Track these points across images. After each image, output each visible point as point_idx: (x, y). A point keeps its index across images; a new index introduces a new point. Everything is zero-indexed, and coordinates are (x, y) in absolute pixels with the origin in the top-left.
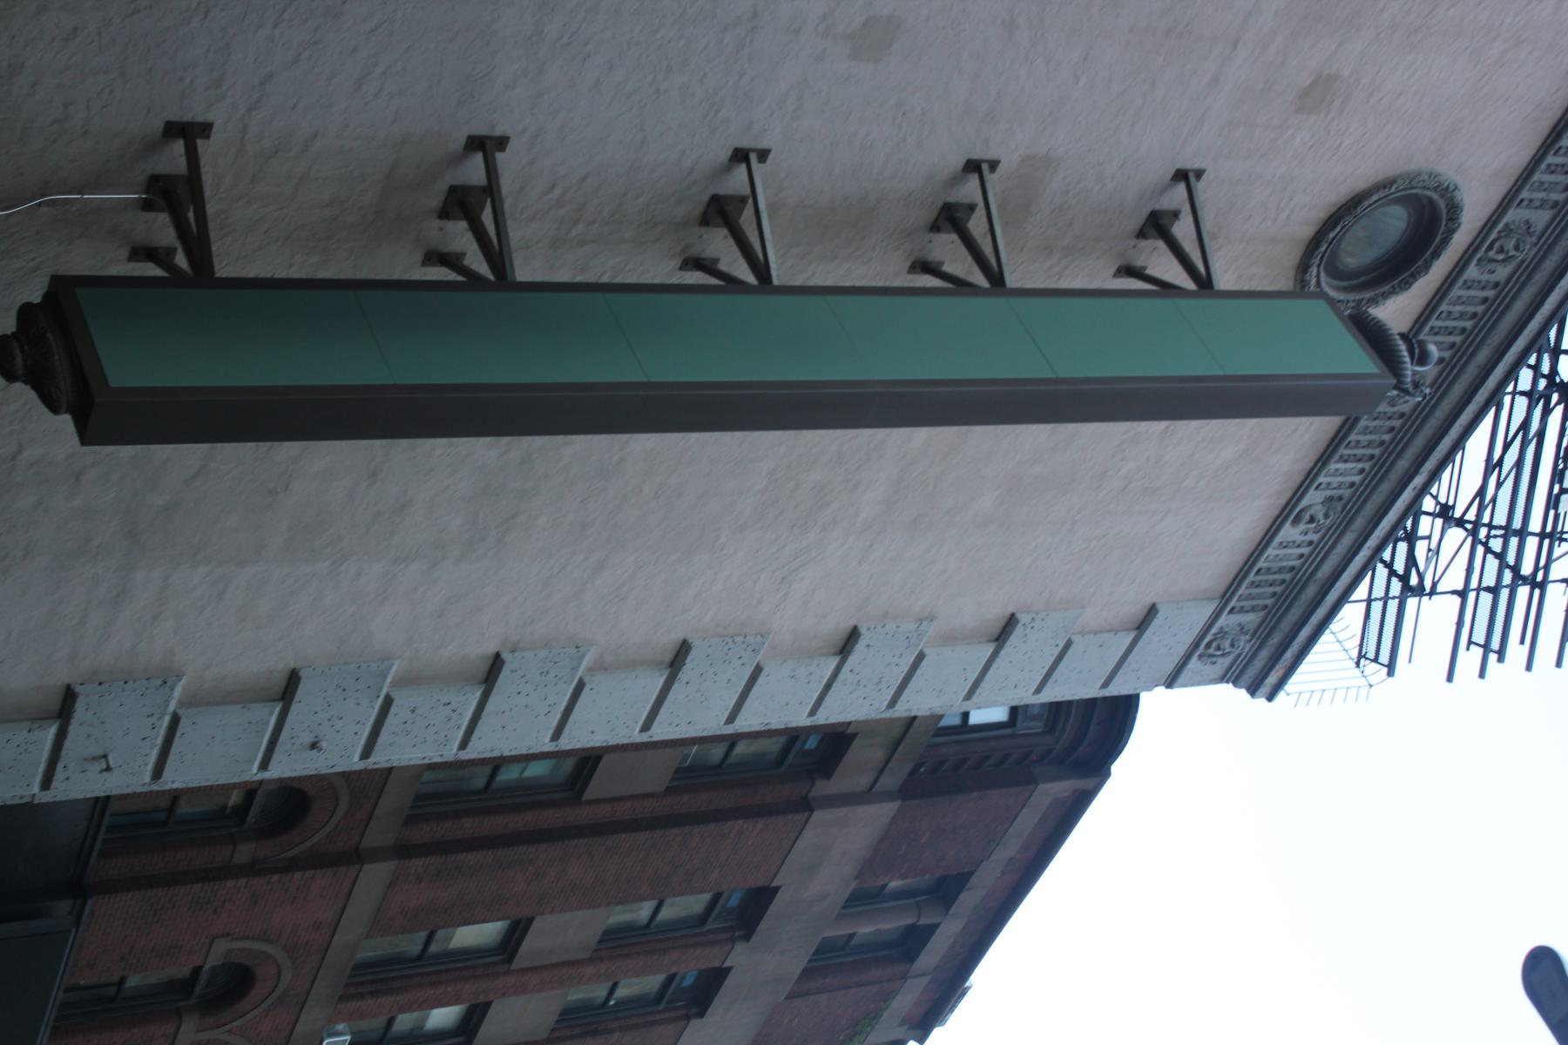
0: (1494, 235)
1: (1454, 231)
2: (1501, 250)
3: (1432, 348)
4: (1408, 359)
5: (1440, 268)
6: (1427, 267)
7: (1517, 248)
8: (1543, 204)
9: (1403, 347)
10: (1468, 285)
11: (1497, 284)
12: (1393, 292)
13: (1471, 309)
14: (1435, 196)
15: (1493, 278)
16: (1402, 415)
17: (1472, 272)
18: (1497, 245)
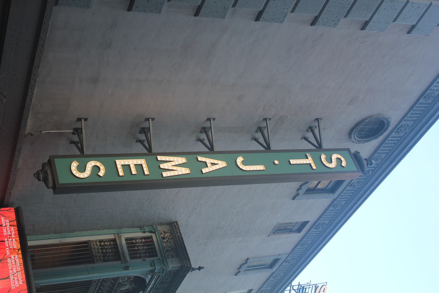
0: (398, 127)
1: (389, 127)
2: (401, 130)
3: (373, 161)
4: (366, 166)
5: (381, 138)
6: (382, 134)
7: (405, 130)
8: (411, 120)
9: (365, 163)
10: (421, 104)
11: (400, 137)
12: (374, 139)
13: (422, 109)
14: (384, 120)
15: (399, 135)
16: (429, 103)
17: (394, 134)
18: (400, 129)
